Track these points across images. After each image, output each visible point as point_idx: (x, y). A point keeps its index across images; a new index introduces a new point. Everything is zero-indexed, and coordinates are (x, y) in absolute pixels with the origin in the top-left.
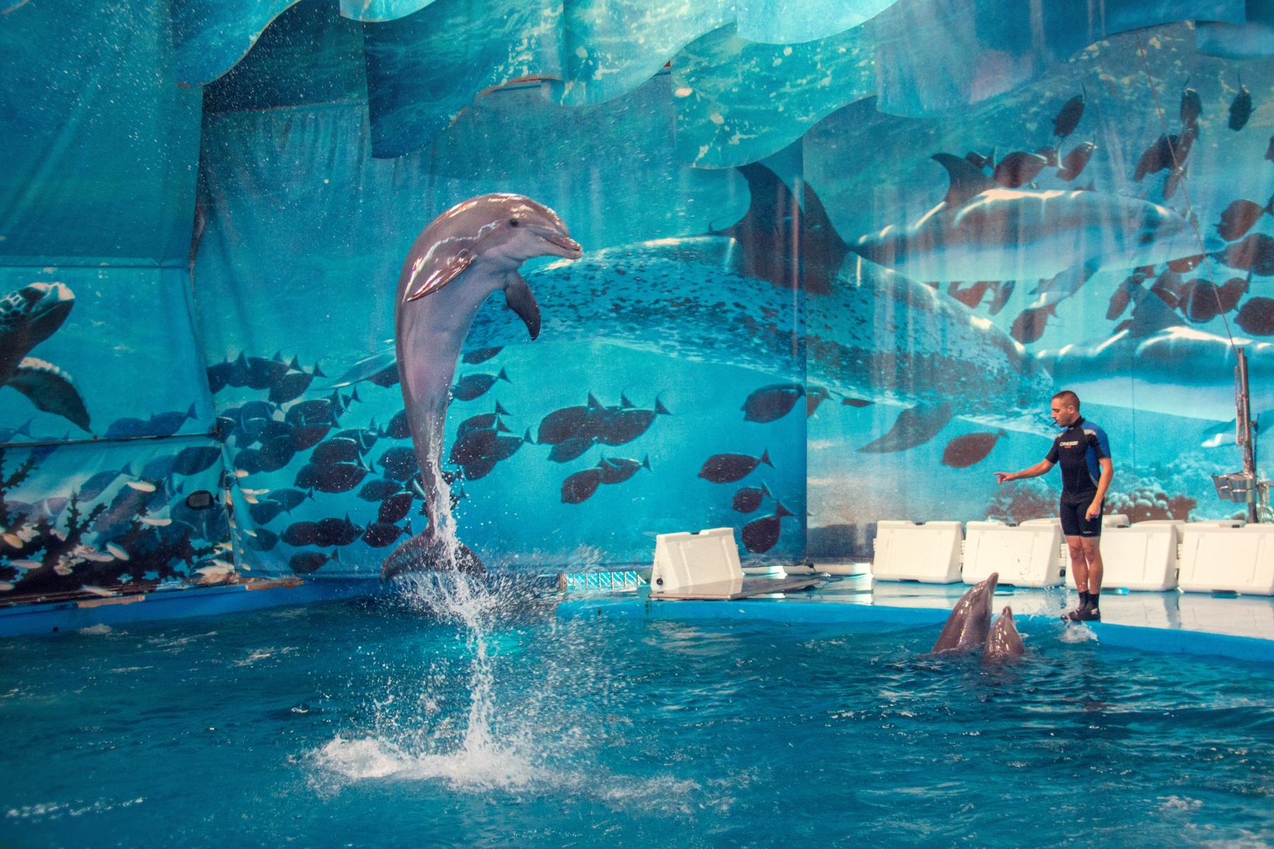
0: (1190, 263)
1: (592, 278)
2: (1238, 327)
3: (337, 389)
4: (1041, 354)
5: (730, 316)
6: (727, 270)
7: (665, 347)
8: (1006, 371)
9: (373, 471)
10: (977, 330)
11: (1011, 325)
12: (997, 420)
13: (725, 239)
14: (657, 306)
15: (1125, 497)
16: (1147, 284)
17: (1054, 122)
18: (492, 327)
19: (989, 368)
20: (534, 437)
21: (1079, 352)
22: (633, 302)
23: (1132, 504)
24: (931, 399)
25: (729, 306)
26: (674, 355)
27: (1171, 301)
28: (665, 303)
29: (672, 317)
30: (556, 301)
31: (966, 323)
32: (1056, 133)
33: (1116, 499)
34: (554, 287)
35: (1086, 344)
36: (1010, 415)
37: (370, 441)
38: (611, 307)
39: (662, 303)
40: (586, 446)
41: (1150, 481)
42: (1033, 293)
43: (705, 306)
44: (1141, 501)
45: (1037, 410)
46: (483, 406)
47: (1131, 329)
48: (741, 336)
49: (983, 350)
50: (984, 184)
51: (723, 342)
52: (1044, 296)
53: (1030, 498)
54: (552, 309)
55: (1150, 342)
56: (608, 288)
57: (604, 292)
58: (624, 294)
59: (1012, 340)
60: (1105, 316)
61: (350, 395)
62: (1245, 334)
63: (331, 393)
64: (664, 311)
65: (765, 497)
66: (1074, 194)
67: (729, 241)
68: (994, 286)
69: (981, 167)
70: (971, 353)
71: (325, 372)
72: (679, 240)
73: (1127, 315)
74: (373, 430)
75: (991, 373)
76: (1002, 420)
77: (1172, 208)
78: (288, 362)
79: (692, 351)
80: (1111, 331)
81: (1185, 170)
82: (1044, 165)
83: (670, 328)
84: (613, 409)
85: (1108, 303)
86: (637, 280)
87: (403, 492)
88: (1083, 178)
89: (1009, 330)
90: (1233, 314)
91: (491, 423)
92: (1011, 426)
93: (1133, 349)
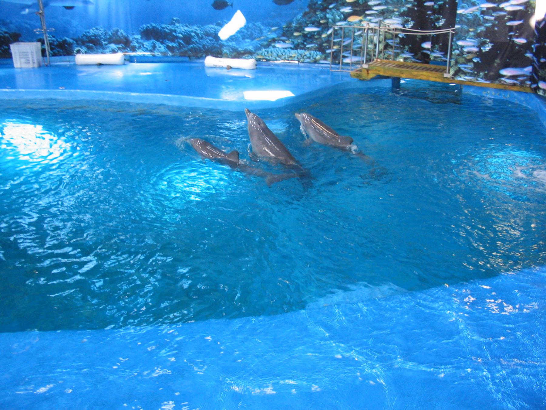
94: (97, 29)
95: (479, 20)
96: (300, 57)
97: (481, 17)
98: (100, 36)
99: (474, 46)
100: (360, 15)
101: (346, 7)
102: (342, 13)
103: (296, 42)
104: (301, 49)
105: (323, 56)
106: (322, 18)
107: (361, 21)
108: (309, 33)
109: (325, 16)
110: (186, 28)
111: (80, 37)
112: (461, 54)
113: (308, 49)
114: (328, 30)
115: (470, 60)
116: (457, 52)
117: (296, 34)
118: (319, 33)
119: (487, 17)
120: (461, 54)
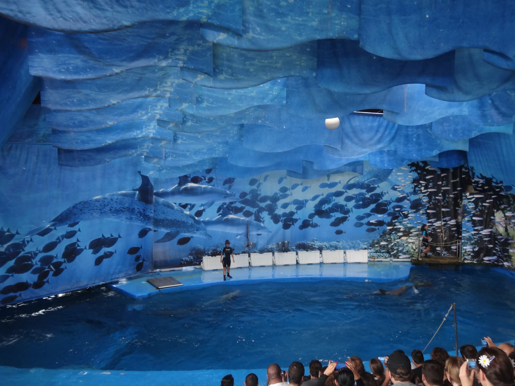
1: (104, 201)
2: (243, 216)
3: (24, 238)
4: (202, 220)
5: (136, 211)
6: (136, 200)
8: (193, 223)
10: (186, 214)
11: (195, 213)
13: (136, 191)
16: (225, 206)
17: (206, 171)
18: (77, 216)
20: (88, 247)
21: (210, 220)
24: (174, 230)
25: (136, 209)
26: (123, 222)
27: (229, 210)
29: (123, 212)
30: (95, 208)
31: (183, 212)
32: (206, 173)
34: (95, 204)
35: (212, 218)
36: (194, 233)
37: (36, 254)
38: (109, 209)
39: (121, 208)
40: (101, 248)
42: (200, 206)
45: (200, 232)
46: (73, 240)
48: (138, 216)
50: (188, 182)
51: (134, 218)
52: (202, 207)
54: (94, 210)
55: (225, 218)
57: (107, 205)
58: (112, 206)
59: (195, 216)
63: (22, 240)
64: (121, 210)
66: (210, 187)
70: (184, 219)
71: (20, 233)
73: (221, 212)
74: (37, 251)
75: (189, 224)
76: (192, 234)
78: (6, 230)
83: (123, 215)
84: (108, 238)
85: (217, 210)
86: (116, 202)
88: (212, 183)
90: (242, 213)
91: (75, 245)
92: (194, 235)
93: (222, 219)
94: (273, 245)
95: (472, 238)
96: (378, 256)
97: (472, 237)
98: (274, 248)
99: (470, 249)
100: (407, 237)
101: (400, 233)
102: (398, 236)
103: (376, 249)
104: (379, 252)
105: (390, 255)
106: (389, 238)
107: (407, 239)
108: (383, 245)
109: (390, 237)
110: (320, 244)
112: (466, 252)
113: (383, 253)
114: (392, 243)
115: (470, 255)
116: (464, 251)
117: (376, 245)
118: (387, 245)
119: (474, 237)
120: (466, 252)
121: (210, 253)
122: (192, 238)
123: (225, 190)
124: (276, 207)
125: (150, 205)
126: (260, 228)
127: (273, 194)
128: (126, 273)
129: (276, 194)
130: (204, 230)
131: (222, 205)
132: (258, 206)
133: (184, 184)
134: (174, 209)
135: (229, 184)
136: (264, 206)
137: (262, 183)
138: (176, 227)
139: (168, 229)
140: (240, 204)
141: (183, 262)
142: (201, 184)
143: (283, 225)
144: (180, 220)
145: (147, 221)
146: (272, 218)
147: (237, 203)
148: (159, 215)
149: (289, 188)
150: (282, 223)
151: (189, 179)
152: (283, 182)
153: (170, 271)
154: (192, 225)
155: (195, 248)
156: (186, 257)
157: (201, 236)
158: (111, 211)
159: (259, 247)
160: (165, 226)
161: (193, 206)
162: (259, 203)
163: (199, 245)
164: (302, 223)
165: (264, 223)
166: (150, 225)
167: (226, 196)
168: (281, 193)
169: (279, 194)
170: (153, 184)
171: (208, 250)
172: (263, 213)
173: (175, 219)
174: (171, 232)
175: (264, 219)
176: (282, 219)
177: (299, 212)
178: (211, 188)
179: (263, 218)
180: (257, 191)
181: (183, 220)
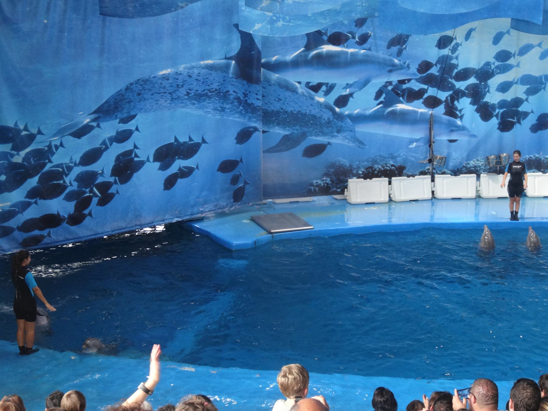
0: (406, 81)
1: (177, 79)
2: (423, 105)
3: (51, 141)
4: (347, 113)
5: (232, 97)
6: (231, 76)
7: (206, 112)
8: (331, 119)
9: (71, 185)
10: (318, 102)
11: (334, 101)
12: (327, 138)
13: (230, 61)
14: (204, 93)
15: (380, 167)
16: (390, 88)
17: (355, 22)
18: (133, 104)
19: (324, 118)
20: (151, 159)
21: (362, 112)
22: (195, 91)
23: (383, 169)
24: (297, 130)
25: (231, 92)
26: (210, 116)
28: (207, 91)
29: (210, 98)
30: (162, 90)
31: (313, 99)
32: (356, 26)
33: (376, 167)
34: (161, 84)
36: (332, 136)
37: (70, 169)
39: (206, 91)
40: (173, 161)
41: (389, 160)
42: (344, 88)
43: (223, 93)
44: (386, 168)
46: (127, 146)
47: (383, 104)
48: (236, 106)
49: (321, 110)
50: (323, 43)
51: (228, 109)
52: (348, 90)
53: (342, 169)
54: (160, 95)
55: (390, 109)
56: (184, 84)
57: (182, 86)
58: (191, 87)
60: (373, 99)
61: (59, 144)
62: (426, 108)
63: (48, 144)
64: (206, 95)
65: (240, 176)
66: (363, 51)
67: (232, 62)
68: (326, 85)
69: (322, 35)
70: (315, 111)
71: (44, 132)
72: (213, 61)
73: (382, 99)
74: (71, 163)
75: (324, 119)
76: (329, 138)
77: (400, 60)
78: (22, 127)
79: (218, 113)
80: (376, 105)
81: (406, 47)
82: (350, 38)
83: (208, 103)
84: (185, 143)
86: (197, 80)
87: (88, 195)
88: (366, 45)
89: (333, 103)
90: (422, 100)
91: (131, 155)
92: (333, 141)
93: (384, 112)
94: (478, 160)
98: (480, 166)
111: (460, 168)
121: (360, 172)
122: (328, 146)
123: (391, 57)
124: (487, 90)
125: (255, 85)
126: (454, 128)
127: (482, 65)
128: (216, 205)
129: (488, 64)
130: (351, 131)
131: (385, 86)
132: (452, 87)
133: (316, 46)
134: (297, 93)
135: (398, 47)
136: (463, 88)
137: (461, 45)
138: (301, 126)
139: (287, 128)
140: (418, 84)
141: (312, 188)
142: (347, 47)
143: (500, 124)
144: (308, 112)
145: (250, 115)
146: (477, 111)
147: (412, 81)
148: (272, 104)
149: (513, 52)
150: (498, 119)
151: (325, 38)
152: (501, 42)
153: (290, 202)
154: (329, 122)
155: (335, 163)
156: (318, 179)
157: (346, 142)
158: (188, 96)
159: (452, 164)
160: (282, 123)
161: (330, 88)
162: (453, 81)
163: (341, 159)
164: (537, 120)
165: (463, 120)
166: (256, 122)
167: (393, 68)
168: (497, 63)
169: (494, 64)
170: (259, 46)
171: (358, 168)
172: (461, 100)
173: (300, 111)
174: (292, 134)
175: (462, 113)
176: (499, 112)
177: (531, 98)
178: (364, 55)
179: (460, 111)
180: (451, 58)
181: (313, 112)
